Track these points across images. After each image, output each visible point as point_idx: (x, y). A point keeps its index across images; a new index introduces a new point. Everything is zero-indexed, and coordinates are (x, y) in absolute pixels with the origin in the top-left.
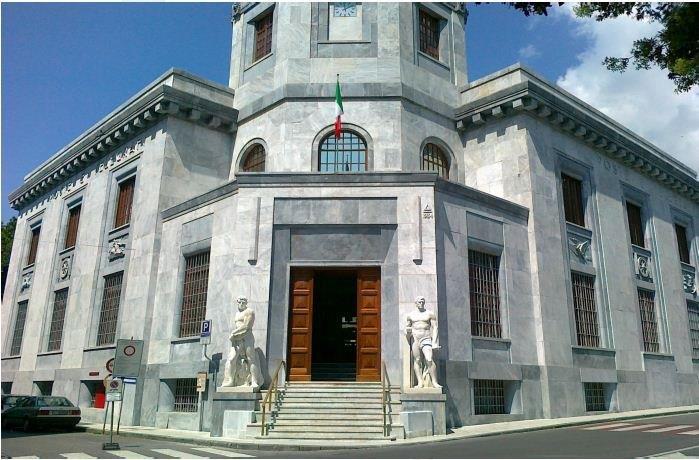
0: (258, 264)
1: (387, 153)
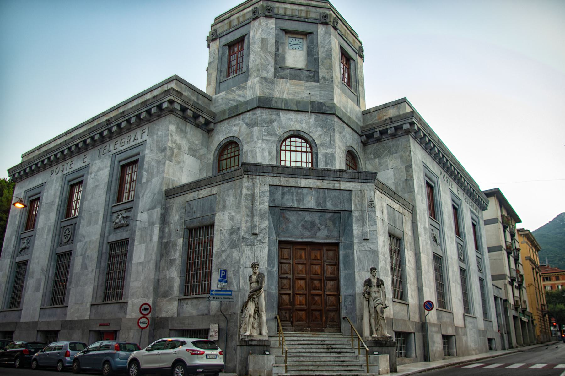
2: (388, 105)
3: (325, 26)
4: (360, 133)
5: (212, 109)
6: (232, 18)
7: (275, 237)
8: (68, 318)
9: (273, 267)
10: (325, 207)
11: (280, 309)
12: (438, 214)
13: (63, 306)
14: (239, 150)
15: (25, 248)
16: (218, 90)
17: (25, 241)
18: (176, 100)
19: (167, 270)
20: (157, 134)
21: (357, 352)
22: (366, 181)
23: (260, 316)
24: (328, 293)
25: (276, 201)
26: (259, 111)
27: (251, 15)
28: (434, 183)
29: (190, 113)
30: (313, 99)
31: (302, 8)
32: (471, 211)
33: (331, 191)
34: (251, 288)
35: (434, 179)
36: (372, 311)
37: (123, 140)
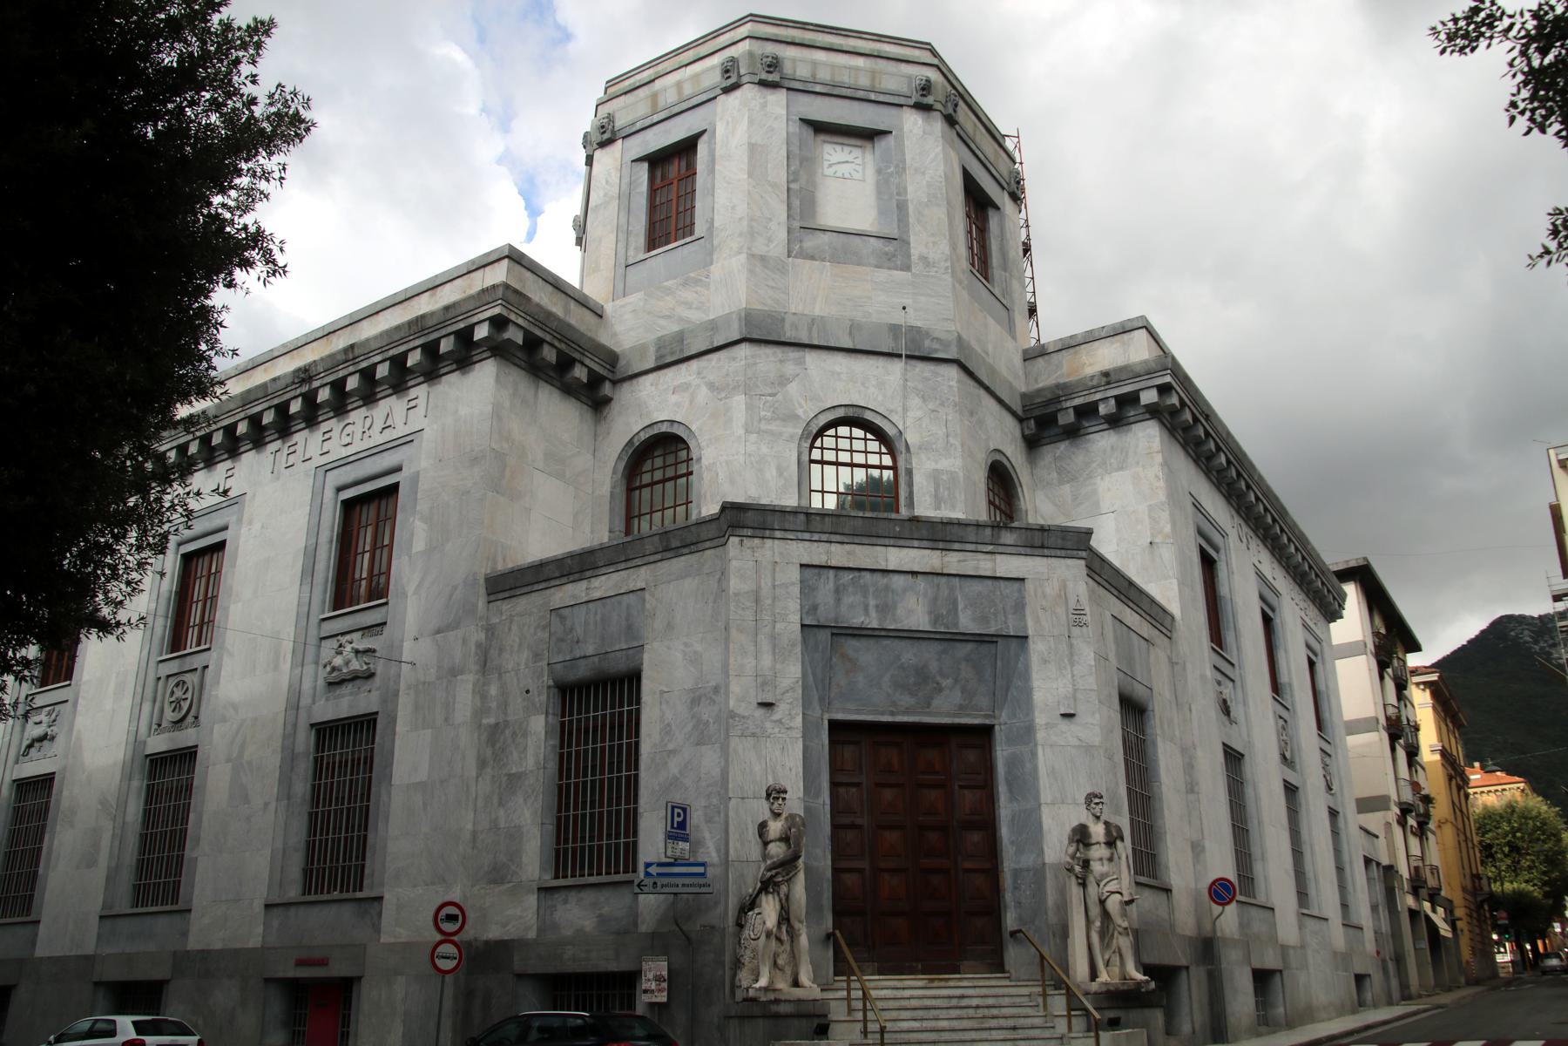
0: (780, 712)
1: (935, 476)
2: (1097, 335)
3: (926, 114)
4: (1020, 412)
5: (605, 339)
6: (658, 84)
7: (818, 713)
8: (193, 944)
9: (818, 794)
10: (956, 625)
11: (837, 914)
12: (1229, 637)
13: (174, 907)
14: (689, 460)
15: (43, 738)
16: (621, 289)
17: (43, 717)
18: (512, 317)
19: (501, 804)
20: (456, 412)
21: (1061, 1027)
22: (1063, 553)
23: (793, 935)
24: (968, 865)
25: (821, 609)
26: (744, 350)
27: (716, 78)
28: (1217, 550)
29: (549, 354)
30: (898, 318)
31: (860, 62)
32: (1306, 626)
33: (969, 582)
34: (765, 857)
35: (1217, 538)
36: (1095, 911)
37: (349, 429)
